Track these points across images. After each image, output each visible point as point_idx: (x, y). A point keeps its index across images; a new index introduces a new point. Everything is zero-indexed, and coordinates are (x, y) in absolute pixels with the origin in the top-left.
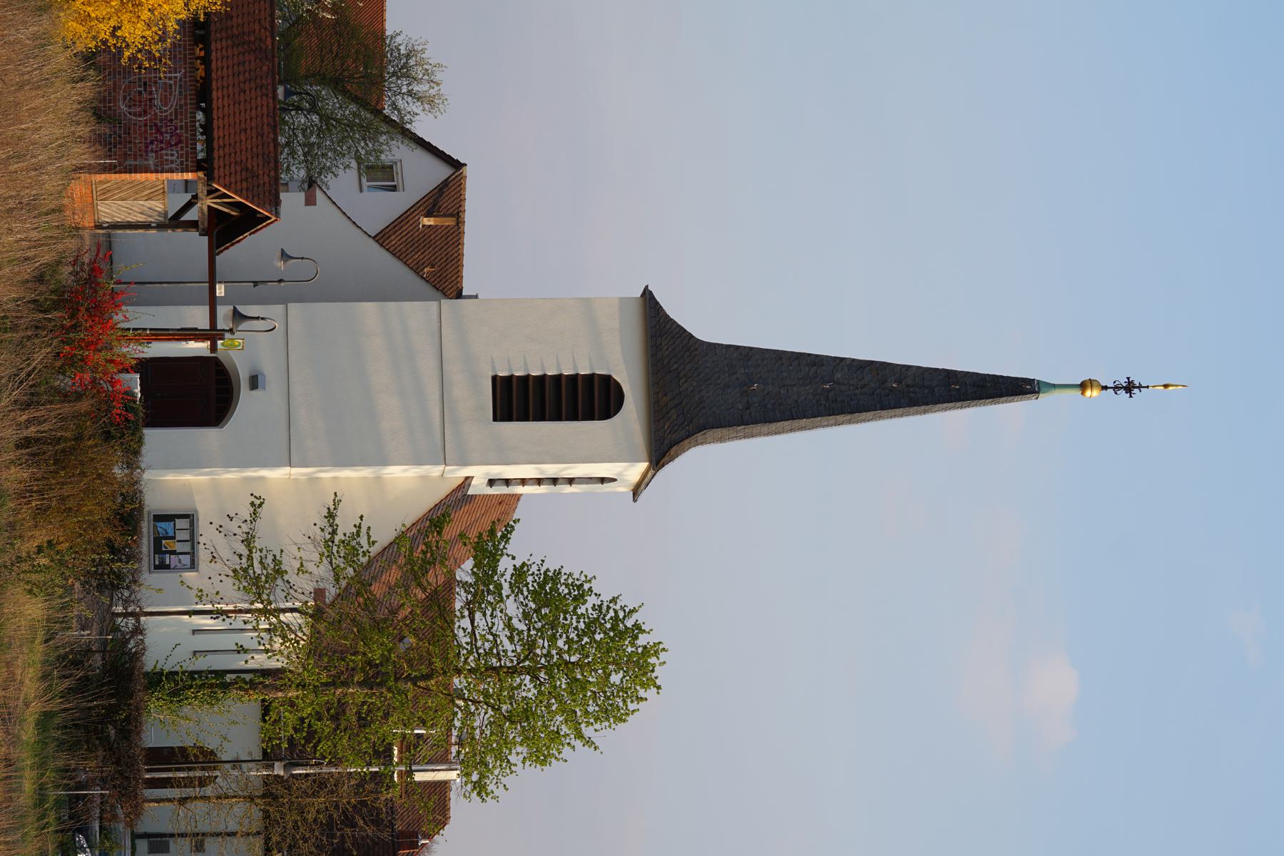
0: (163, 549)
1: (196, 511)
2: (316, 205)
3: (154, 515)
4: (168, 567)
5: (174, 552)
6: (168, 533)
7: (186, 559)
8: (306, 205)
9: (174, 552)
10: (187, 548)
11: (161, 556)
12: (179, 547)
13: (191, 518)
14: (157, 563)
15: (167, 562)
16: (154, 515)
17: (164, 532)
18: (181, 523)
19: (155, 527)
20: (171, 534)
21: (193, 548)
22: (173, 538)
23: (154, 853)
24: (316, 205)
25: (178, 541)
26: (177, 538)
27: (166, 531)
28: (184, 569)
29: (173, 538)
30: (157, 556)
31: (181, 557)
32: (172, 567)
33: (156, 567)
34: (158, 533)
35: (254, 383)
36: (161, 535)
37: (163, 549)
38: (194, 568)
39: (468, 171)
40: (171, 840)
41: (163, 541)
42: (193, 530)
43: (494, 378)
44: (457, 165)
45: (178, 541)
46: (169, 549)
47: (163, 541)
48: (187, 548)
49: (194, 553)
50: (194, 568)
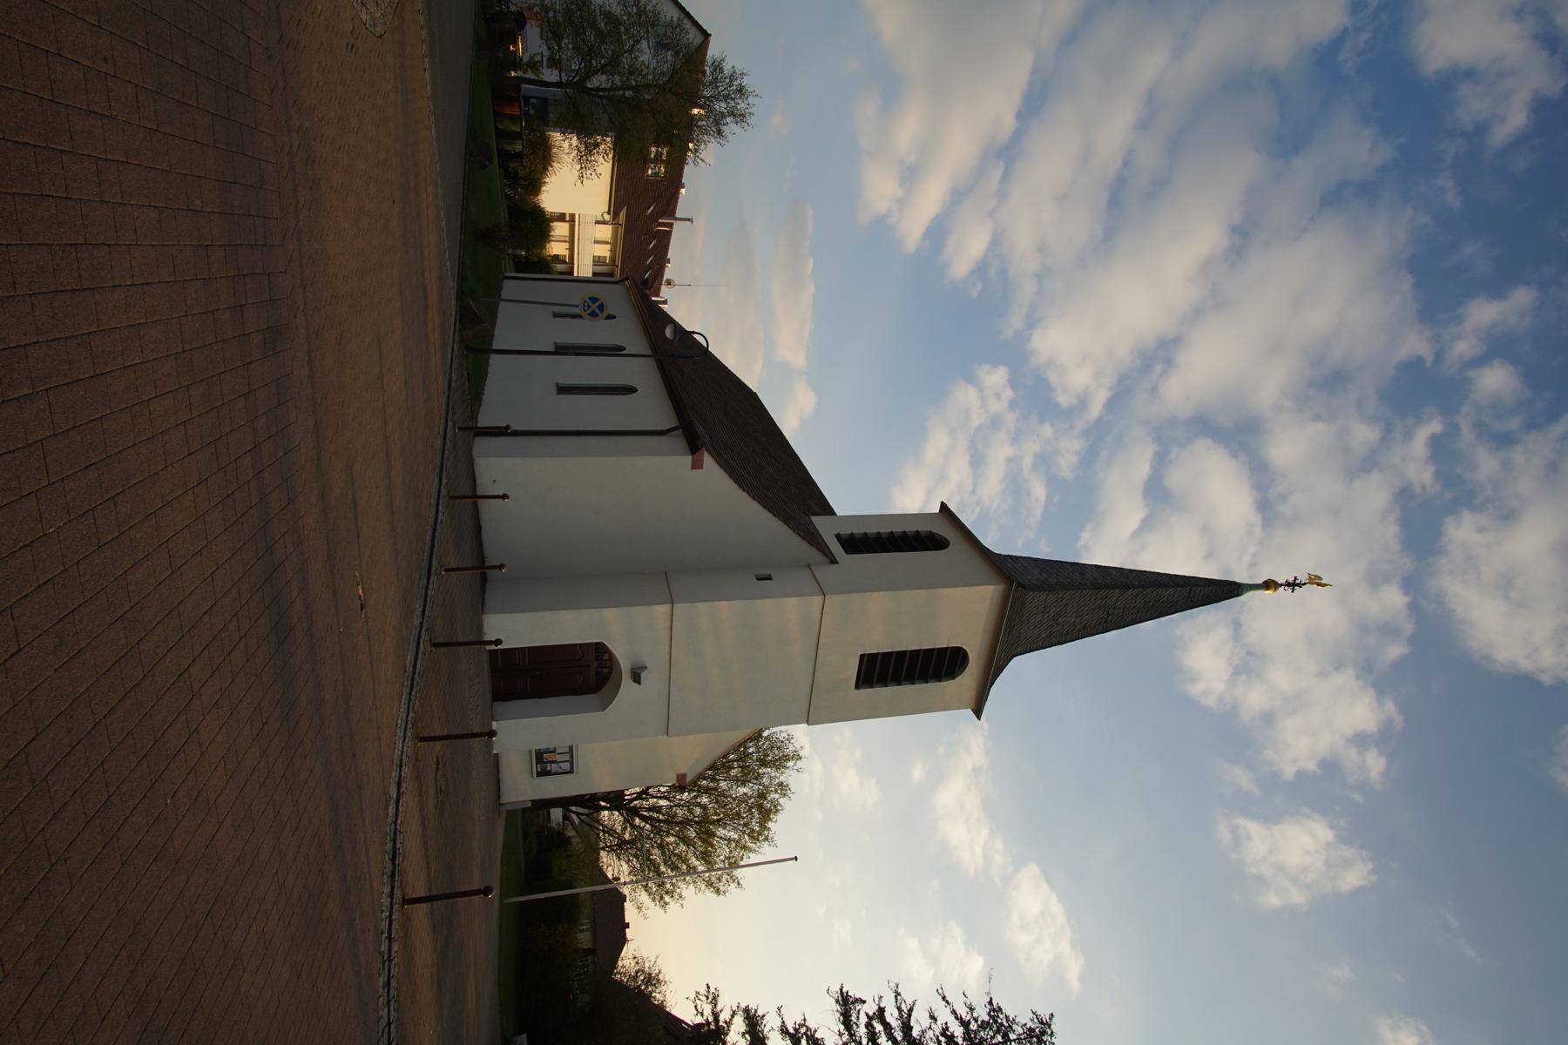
0: (545, 760)
2: (702, 468)
4: (549, 773)
5: (555, 762)
8: (693, 468)
9: (555, 762)
10: (567, 757)
12: (558, 758)
14: (539, 770)
15: (549, 769)
21: (572, 756)
24: (702, 468)
26: (557, 751)
30: (539, 765)
31: (561, 764)
32: (553, 771)
33: (539, 774)
35: (636, 678)
39: (712, 39)
43: (862, 656)
44: (706, 35)
50: (573, 772)
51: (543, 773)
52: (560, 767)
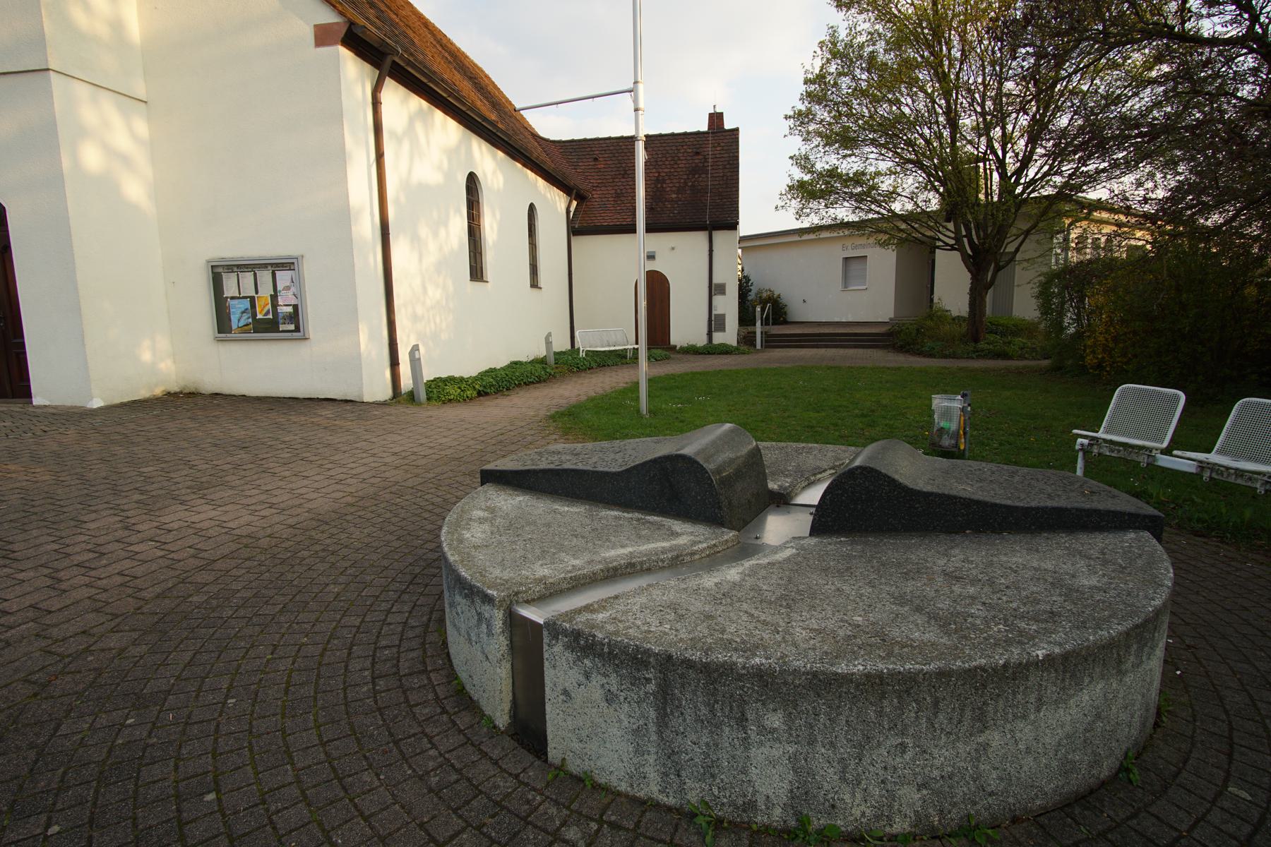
0: (271, 317)
1: (208, 262)
3: (219, 332)
5: (274, 297)
6: (247, 309)
7: (283, 277)
9: (274, 297)
11: (281, 321)
12: (266, 291)
13: (220, 270)
14: (292, 327)
15: (290, 309)
16: (219, 332)
17: (245, 316)
18: (230, 288)
19: (244, 329)
20: (247, 304)
22: (252, 299)
23: (725, 328)
25: (257, 292)
26: (253, 294)
27: (243, 312)
28: (298, 282)
29: (252, 299)
30: (282, 327)
33: (297, 329)
34: (247, 325)
36: (250, 320)
37: (271, 317)
38: (293, 263)
40: (714, 312)
41: (259, 316)
42: (238, 266)
45: (257, 292)
46: (269, 306)
47: (259, 316)
48: (264, 276)
49: (272, 265)
51: (295, 316)
52: (287, 288)
